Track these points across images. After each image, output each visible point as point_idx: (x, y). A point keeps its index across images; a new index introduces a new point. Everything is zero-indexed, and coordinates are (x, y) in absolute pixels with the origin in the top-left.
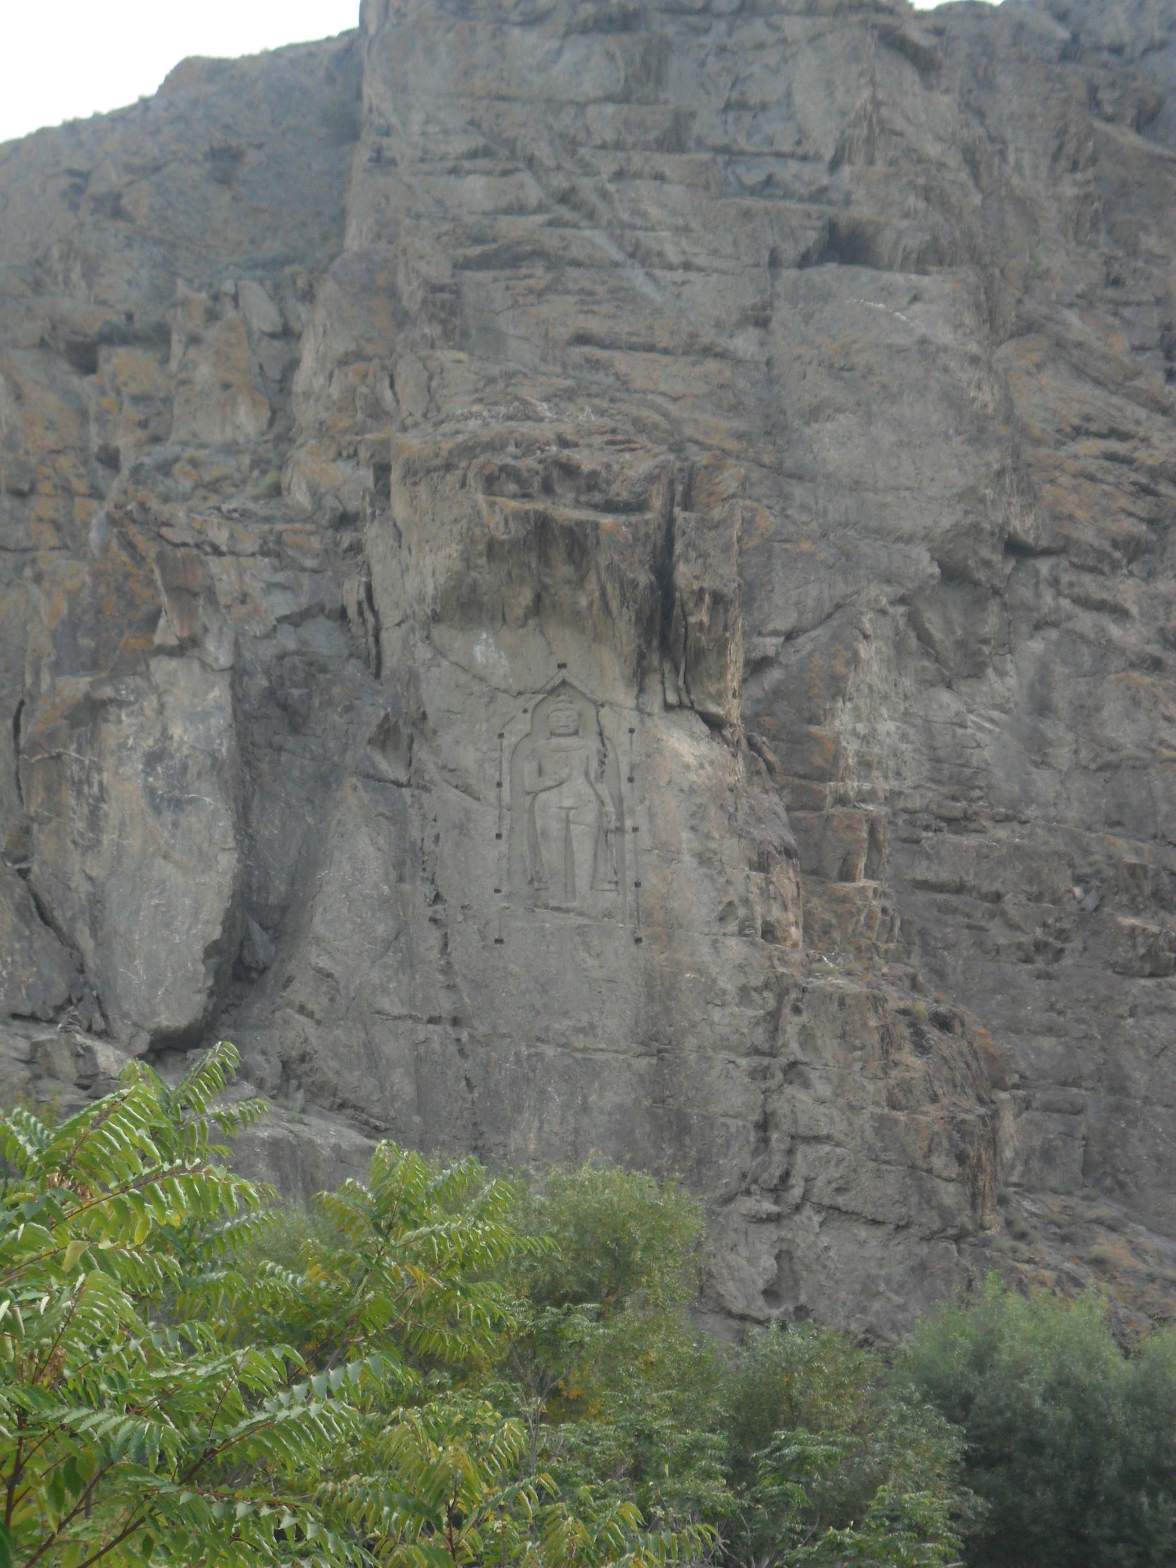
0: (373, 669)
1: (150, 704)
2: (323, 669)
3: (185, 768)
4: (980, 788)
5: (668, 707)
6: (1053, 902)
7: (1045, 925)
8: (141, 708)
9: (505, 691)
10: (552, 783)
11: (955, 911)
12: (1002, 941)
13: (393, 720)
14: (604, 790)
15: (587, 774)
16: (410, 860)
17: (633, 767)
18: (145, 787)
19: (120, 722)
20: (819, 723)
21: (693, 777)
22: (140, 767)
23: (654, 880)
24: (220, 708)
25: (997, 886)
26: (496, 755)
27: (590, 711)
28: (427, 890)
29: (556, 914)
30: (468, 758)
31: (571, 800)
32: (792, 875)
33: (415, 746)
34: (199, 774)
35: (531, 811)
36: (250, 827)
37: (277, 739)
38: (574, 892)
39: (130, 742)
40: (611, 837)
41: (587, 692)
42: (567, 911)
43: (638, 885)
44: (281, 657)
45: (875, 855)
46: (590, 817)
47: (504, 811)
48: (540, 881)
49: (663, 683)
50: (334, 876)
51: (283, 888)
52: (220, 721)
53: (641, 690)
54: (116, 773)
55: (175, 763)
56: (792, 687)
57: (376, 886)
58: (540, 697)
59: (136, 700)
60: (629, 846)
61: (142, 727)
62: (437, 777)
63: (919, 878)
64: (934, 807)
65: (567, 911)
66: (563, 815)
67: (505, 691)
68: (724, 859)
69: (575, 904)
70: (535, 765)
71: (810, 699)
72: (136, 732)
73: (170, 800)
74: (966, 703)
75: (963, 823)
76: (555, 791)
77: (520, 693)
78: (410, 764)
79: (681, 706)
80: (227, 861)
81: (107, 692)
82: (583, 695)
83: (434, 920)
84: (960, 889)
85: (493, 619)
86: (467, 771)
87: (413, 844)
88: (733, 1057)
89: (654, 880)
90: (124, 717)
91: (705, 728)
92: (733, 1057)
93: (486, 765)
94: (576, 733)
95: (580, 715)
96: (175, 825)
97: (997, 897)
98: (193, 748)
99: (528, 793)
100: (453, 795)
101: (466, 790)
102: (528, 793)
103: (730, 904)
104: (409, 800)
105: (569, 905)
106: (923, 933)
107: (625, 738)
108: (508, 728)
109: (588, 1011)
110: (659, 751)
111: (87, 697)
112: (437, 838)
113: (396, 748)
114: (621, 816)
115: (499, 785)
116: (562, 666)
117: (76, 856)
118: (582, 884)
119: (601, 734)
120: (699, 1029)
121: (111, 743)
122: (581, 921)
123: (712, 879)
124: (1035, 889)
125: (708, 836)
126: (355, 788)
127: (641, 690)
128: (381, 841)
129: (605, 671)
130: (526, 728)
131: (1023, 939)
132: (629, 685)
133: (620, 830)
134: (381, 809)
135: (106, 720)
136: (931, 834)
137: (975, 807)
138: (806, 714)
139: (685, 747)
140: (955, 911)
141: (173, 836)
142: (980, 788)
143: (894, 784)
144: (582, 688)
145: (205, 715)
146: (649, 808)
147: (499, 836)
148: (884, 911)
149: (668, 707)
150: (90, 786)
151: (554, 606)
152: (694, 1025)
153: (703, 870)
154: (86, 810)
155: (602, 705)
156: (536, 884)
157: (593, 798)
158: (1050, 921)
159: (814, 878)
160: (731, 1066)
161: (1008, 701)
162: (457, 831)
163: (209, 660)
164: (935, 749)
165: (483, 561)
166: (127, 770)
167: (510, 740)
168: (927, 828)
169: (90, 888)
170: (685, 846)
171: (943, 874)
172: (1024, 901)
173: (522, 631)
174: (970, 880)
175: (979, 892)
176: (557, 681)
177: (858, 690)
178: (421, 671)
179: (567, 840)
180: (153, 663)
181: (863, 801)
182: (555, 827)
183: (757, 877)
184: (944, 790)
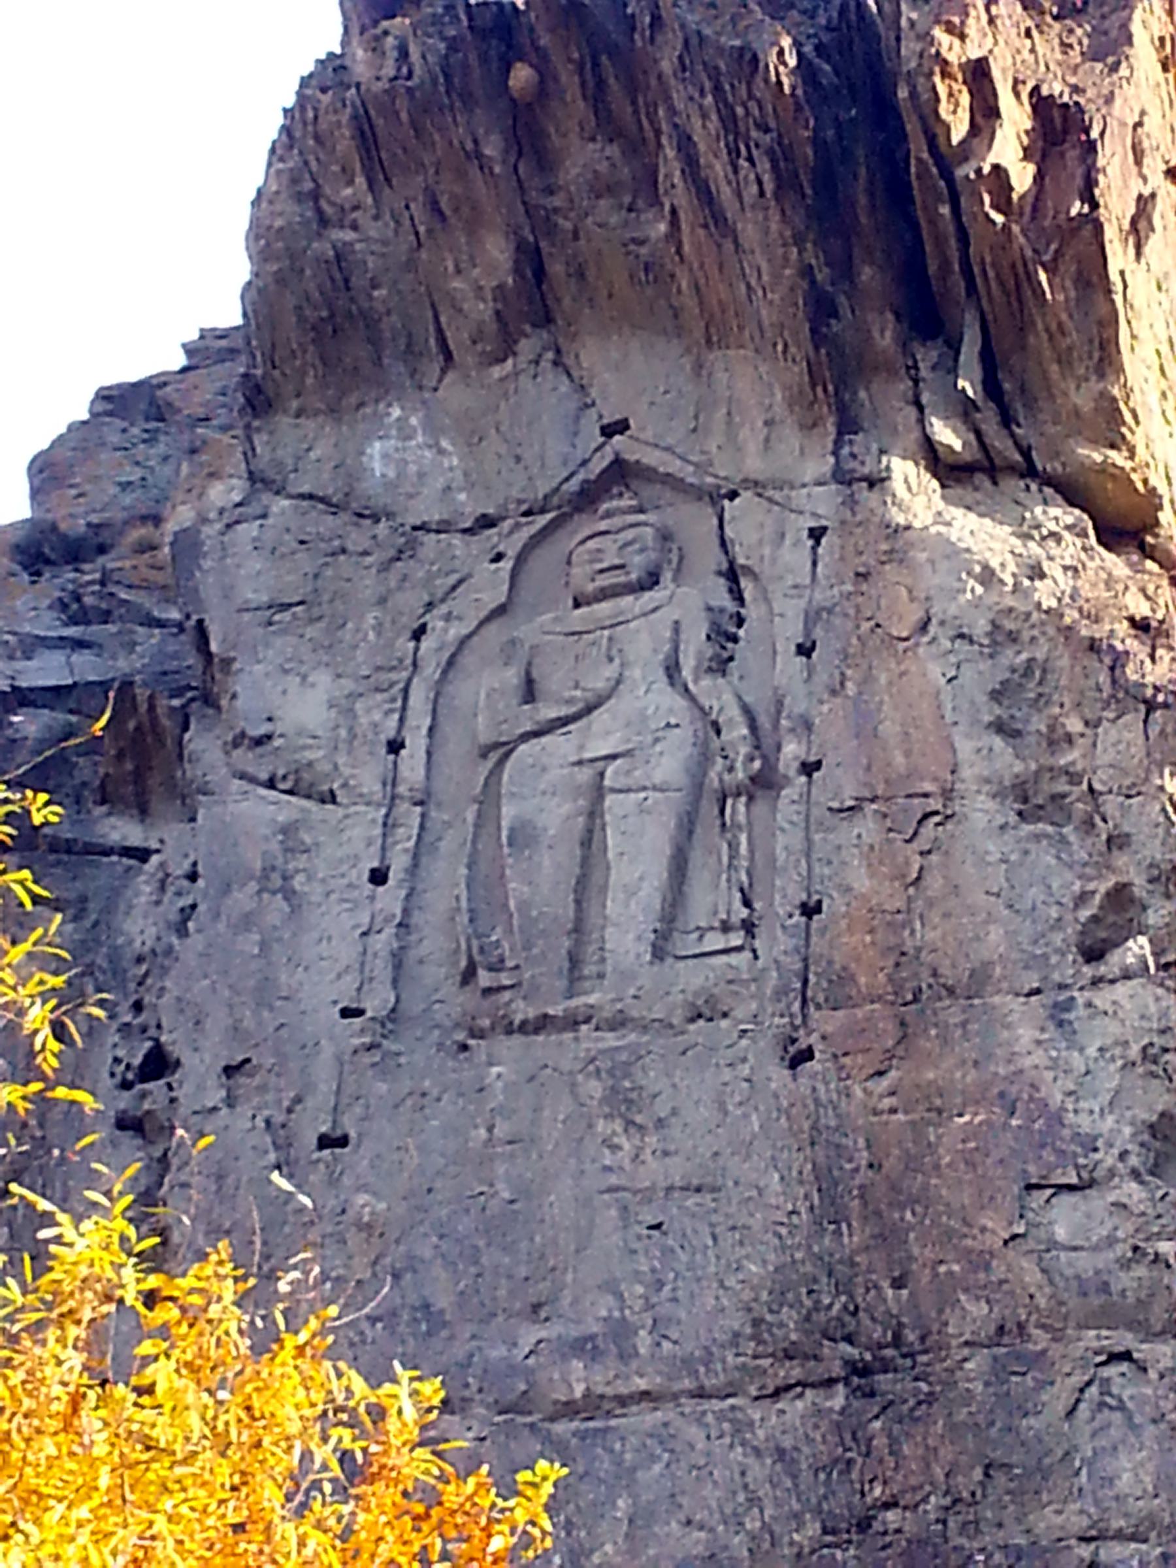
9: (443, 528)
10: (564, 711)
15: (672, 670)
40: (738, 809)
41: (688, 474)
42: (572, 1022)
46: (669, 763)
47: (403, 807)
48: (496, 967)
53: (847, 426)
58: (542, 520)
65: (572, 1022)
66: (585, 775)
67: (443, 528)
69: (592, 999)
70: (512, 676)
83: (130, 1124)
85: (411, 352)
88: (1125, 1340)
92: (1125, 1340)
93: (359, 706)
95: (665, 536)
101: (299, 785)
107: (795, 556)
109: (611, 1287)
115: (395, 747)
120: (999, 1270)
122: (610, 1040)
127: (847, 426)
129: (742, 414)
132: (810, 426)
144: (674, 466)
147: (378, 877)
151: (581, 275)
152: (980, 1261)
153: (1027, 828)
155: (733, 495)
156: (484, 978)
160: (1112, 1371)
165: (355, 190)
167: (443, 633)
170: (966, 772)
173: (497, 372)
179: (590, 840)
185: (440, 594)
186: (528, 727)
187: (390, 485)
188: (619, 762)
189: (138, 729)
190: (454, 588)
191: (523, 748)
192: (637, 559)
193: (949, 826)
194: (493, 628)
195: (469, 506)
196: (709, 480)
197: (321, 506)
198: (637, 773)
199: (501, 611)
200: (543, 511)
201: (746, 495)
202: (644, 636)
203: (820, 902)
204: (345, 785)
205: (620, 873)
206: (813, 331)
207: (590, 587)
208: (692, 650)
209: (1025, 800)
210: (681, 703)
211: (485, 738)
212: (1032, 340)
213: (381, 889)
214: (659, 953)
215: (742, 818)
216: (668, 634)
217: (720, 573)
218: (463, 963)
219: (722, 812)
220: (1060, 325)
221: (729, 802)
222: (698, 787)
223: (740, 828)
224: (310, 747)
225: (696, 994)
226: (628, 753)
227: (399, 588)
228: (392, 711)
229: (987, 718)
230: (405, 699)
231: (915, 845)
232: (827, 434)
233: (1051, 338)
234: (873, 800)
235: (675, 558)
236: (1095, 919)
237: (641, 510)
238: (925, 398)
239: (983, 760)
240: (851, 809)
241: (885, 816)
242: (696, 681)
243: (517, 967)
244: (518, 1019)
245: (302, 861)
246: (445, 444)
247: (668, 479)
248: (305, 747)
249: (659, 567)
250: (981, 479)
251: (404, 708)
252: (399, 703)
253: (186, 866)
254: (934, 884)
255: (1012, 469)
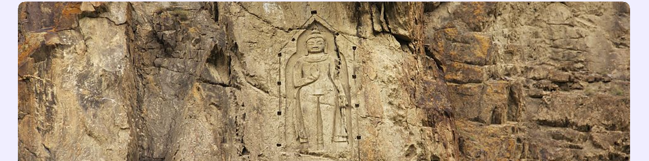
0: (213, 16)
1: (80, 45)
2: (184, 18)
3: (100, 82)
4: (582, 62)
5: (375, 33)
6: (622, 130)
7: (616, 144)
8: (75, 48)
10: (310, 81)
11: (563, 138)
12: (590, 155)
13: (219, 48)
14: (340, 83)
15: (329, 75)
16: (229, 131)
17: (355, 69)
18: (78, 94)
19: (63, 57)
20: (480, 31)
21: (389, 73)
22: (75, 83)
23: (368, 135)
24: (120, 47)
25: (587, 122)
26: (277, 66)
27: (330, 38)
28: (238, 145)
29: (313, 157)
30: (260, 68)
31: (321, 89)
32: (449, 127)
33: (232, 63)
34: (108, 85)
35: (298, 98)
36: (142, 113)
37: (158, 61)
38: (322, 143)
39: (69, 68)
41: (329, 27)
42: (319, 155)
43: (359, 138)
44: (159, 13)
45: (514, 107)
46: (331, 100)
49: (372, 19)
50: (185, 142)
51: (161, 148)
52: (120, 54)
53: (359, 25)
54: (61, 87)
55: (95, 79)
56: (464, 10)
57: (210, 146)
59: (72, 44)
60: (353, 116)
61: (76, 60)
62: (243, 80)
63: (541, 119)
64: (551, 75)
65: (319, 155)
67: (282, 29)
68: (408, 120)
69: (323, 151)
71: (474, 17)
72: (73, 63)
73: (92, 102)
74: (573, 11)
75: (569, 84)
76: (311, 85)
77: (290, 29)
78: (230, 73)
79: (384, 32)
80: (125, 136)
81: (55, 40)
82: (327, 29)
84: (566, 124)
86: (260, 76)
87: (231, 120)
89: (368, 135)
90: (65, 55)
91: (398, 44)
93: (271, 72)
94: (323, 51)
96: (95, 116)
97: (588, 128)
98: (104, 70)
99: (296, 88)
100: (253, 91)
101: (260, 87)
102: (296, 88)
103: (412, 146)
104: (229, 94)
105: (320, 151)
106: (543, 151)
107: (351, 53)
108: (284, 50)
110: (370, 59)
111: (43, 44)
112: (244, 116)
113: (223, 64)
114: (349, 101)
115: (279, 83)
116: (314, 12)
117: (39, 136)
118: (327, 139)
119: (337, 50)
121: (58, 70)
123: (401, 131)
124: (610, 122)
125: (399, 107)
126: (198, 89)
127: (359, 25)
128: (212, 119)
130: (294, 50)
131: (602, 153)
132: (352, 22)
133: (348, 106)
134: (212, 100)
135: (55, 57)
136: (548, 93)
137: (577, 74)
138: (473, 26)
139: (386, 57)
140: (563, 138)
141: (94, 123)
142: (582, 62)
143: (528, 64)
144: (326, 25)
145: (112, 50)
146: (365, 93)
147: (279, 113)
148: (519, 140)
149: (375, 33)
150: (47, 95)
153: (395, 128)
154: (44, 109)
156: (301, 140)
157: (333, 88)
158: (619, 141)
159: (475, 123)
161: (600, 8)
162: (255, 112)
163: (113, 19)
164: (554, 40)
166: (67, 85)
168: (546, 89)
169: (48, 155)
170: (385, 114)
171: (556, 116)
172: (604, 130)
174: (572, 119)
175: (576, 126)
176: (311, 21)
177: (504, 9)
178: (234, 19)
179: (319, 113)
180: (81, 22)
181: (508, 75)
182: (311, 107)
183: (428, 130)
184: (558, 65)
185: (283, 46)
186: (304, 84)
187: (270, 15)
188: (322, 96)
189: (218, 53)
190: (285, 45)
191: (303, 88)
192: (320, 46)
193: (382, 125)
194: (293, 57)
195: (288, 26)
196: (333, 29)
197: (256, 17)
198: (326, 100)
199: (296, 53)
200: (301, 28)
201: (340, 35)
202: (323, 66)
203: (360, 137)
204: (270, 91)
205: (325, 123)
206: (356, 9)
207: (312, 51)
208: (333, 72)
209: (395, 120)
210: (332, 85)
211: (296, 85)
212: (393, 9)
213: (280, 116)
214: (332, 141)
215: (345, 114)
216: (328, 67)
217: (335, 50)
218: (297, 137)
219: (341, 110)
220: (399, 8)
221: (342, 109)
222: (337, 105)
223: (345, 115)
224: (262, 80)
225: (341, 153)
226: (323, 95)
227: (275, 43)
228: (277, 75)
229: (388, 101)
230: (280, 72)
231: (376, 129)
232: (355, 25)
233: (397, 10)
234: (369, 116)
235: (326, 44)
236: (408, 150)
237: (320, 33)
238: (374, 20)
239: (387, 111)
240: (365, 117)
241: (371, 120)
242: (334, 79)
243: (307, 139)
244: (309, 152)
245: (264, 108)
246: (280, 7)
247: (325, 27)
248: (262, 80)
249: (324, 47)
250: (382, 34)
251: (280, 74)
252: (278, 74)
253: (242, 103)
254: (380, 137)
255: (388, 33)
